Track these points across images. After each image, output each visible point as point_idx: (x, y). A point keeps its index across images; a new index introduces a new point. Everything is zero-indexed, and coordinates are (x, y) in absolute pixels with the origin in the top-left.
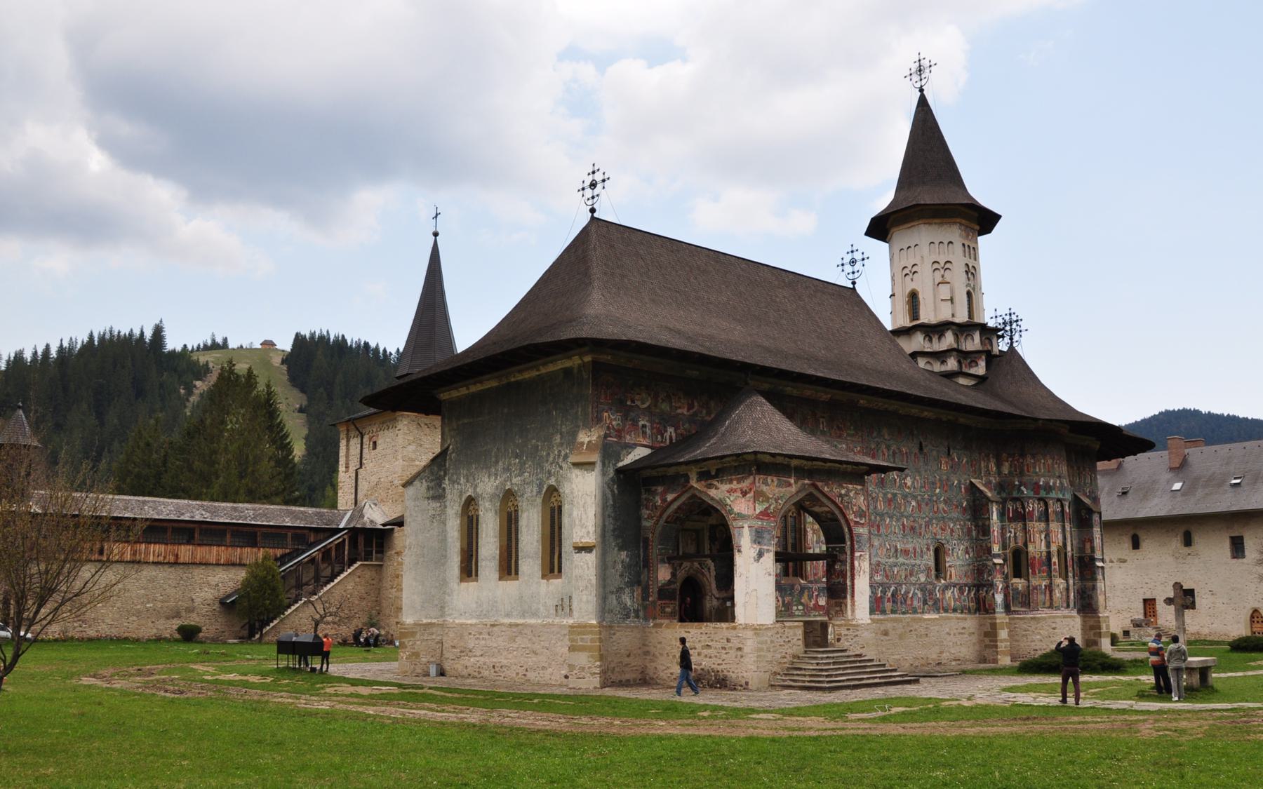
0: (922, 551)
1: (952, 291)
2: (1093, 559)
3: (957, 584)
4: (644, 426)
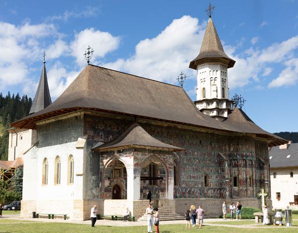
1: (217, 87)
2: (264, 181)
4: (101, 135)
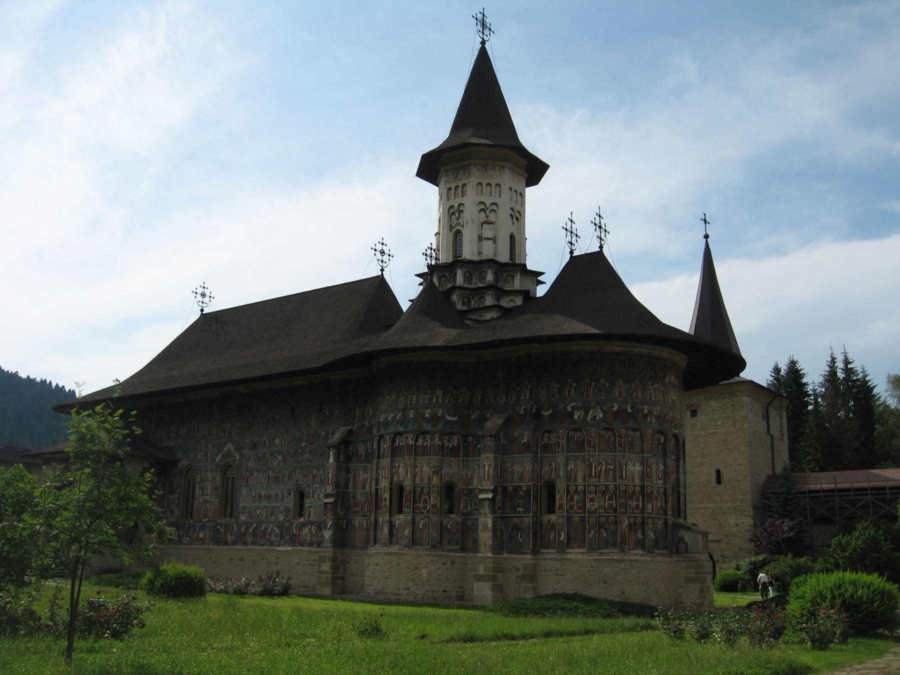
0: (283, 496)
3: (316, 522)
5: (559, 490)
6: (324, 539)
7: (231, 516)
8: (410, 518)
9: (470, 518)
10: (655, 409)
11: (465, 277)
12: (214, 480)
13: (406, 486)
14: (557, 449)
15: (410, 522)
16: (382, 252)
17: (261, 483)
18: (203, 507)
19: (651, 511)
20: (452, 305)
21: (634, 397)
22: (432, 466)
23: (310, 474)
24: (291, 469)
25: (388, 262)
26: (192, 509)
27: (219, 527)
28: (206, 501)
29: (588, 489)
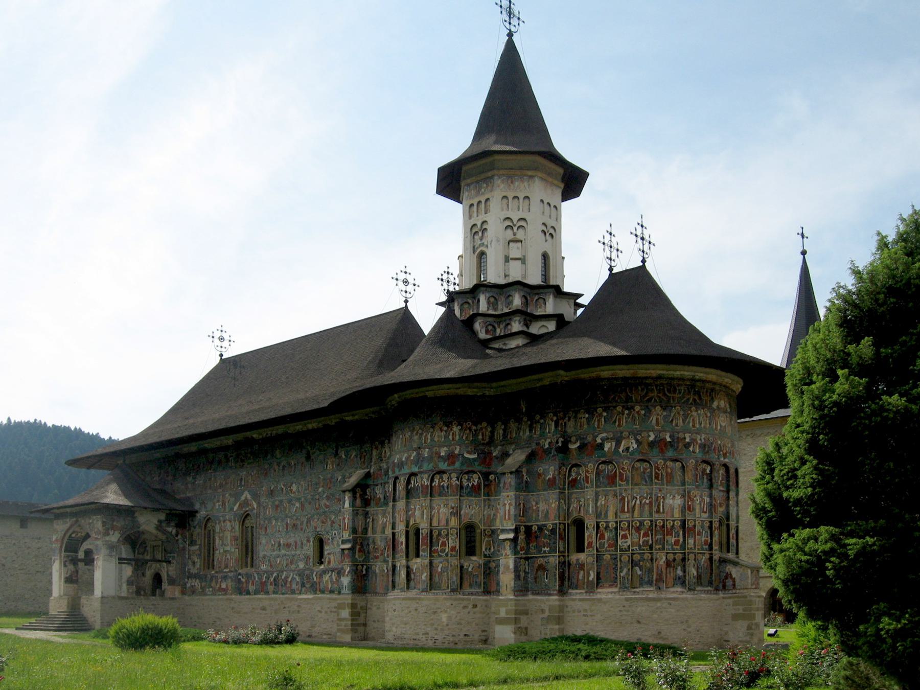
0: (302, 544)
3: (336, 569)
5: (588, 528)
6: (343, 586)
7: (252, 566)
8: (427, 561)
9: (493, 561)
10: (699, 437)
11: (488, 303)
12: (233, 530)
13: (422, 529)
14: (586, 484)
15: (427, 566)
16: (406, 282)
17: (279, 531)
18: (224, 557)
19: (693, 547)
20: (474, 333)
21: (674, 425)
22: (449, 506)
23: (328, 520)
24: (309, 515)
25: (412, 292)
26: (213, 560)
27: (240, 577)
28: (226, 551)
29: (620, 525)
